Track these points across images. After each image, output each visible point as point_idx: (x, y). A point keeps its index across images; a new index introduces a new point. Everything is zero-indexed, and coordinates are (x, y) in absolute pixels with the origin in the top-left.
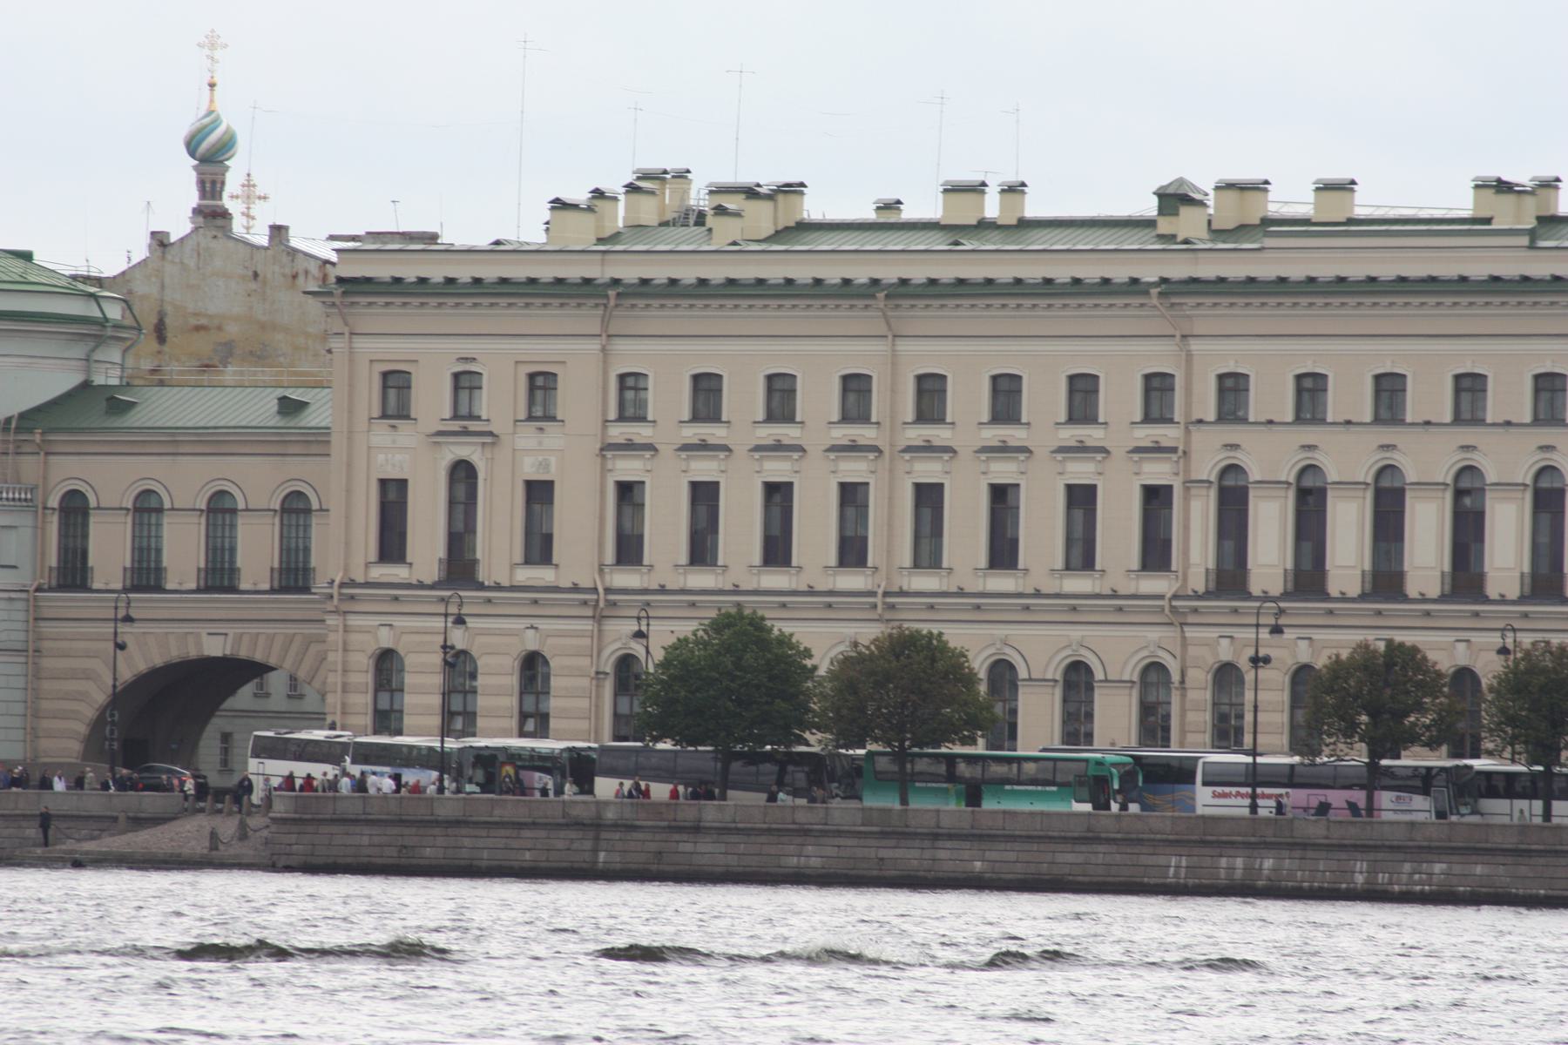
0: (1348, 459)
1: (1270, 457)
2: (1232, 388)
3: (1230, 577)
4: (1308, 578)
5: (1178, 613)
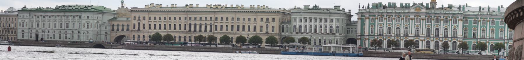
0: (198, 23)
1: (193, 22)
2: (190, 18)
3: (190, 30)
4: (195, 30)
5: (187, 33)
